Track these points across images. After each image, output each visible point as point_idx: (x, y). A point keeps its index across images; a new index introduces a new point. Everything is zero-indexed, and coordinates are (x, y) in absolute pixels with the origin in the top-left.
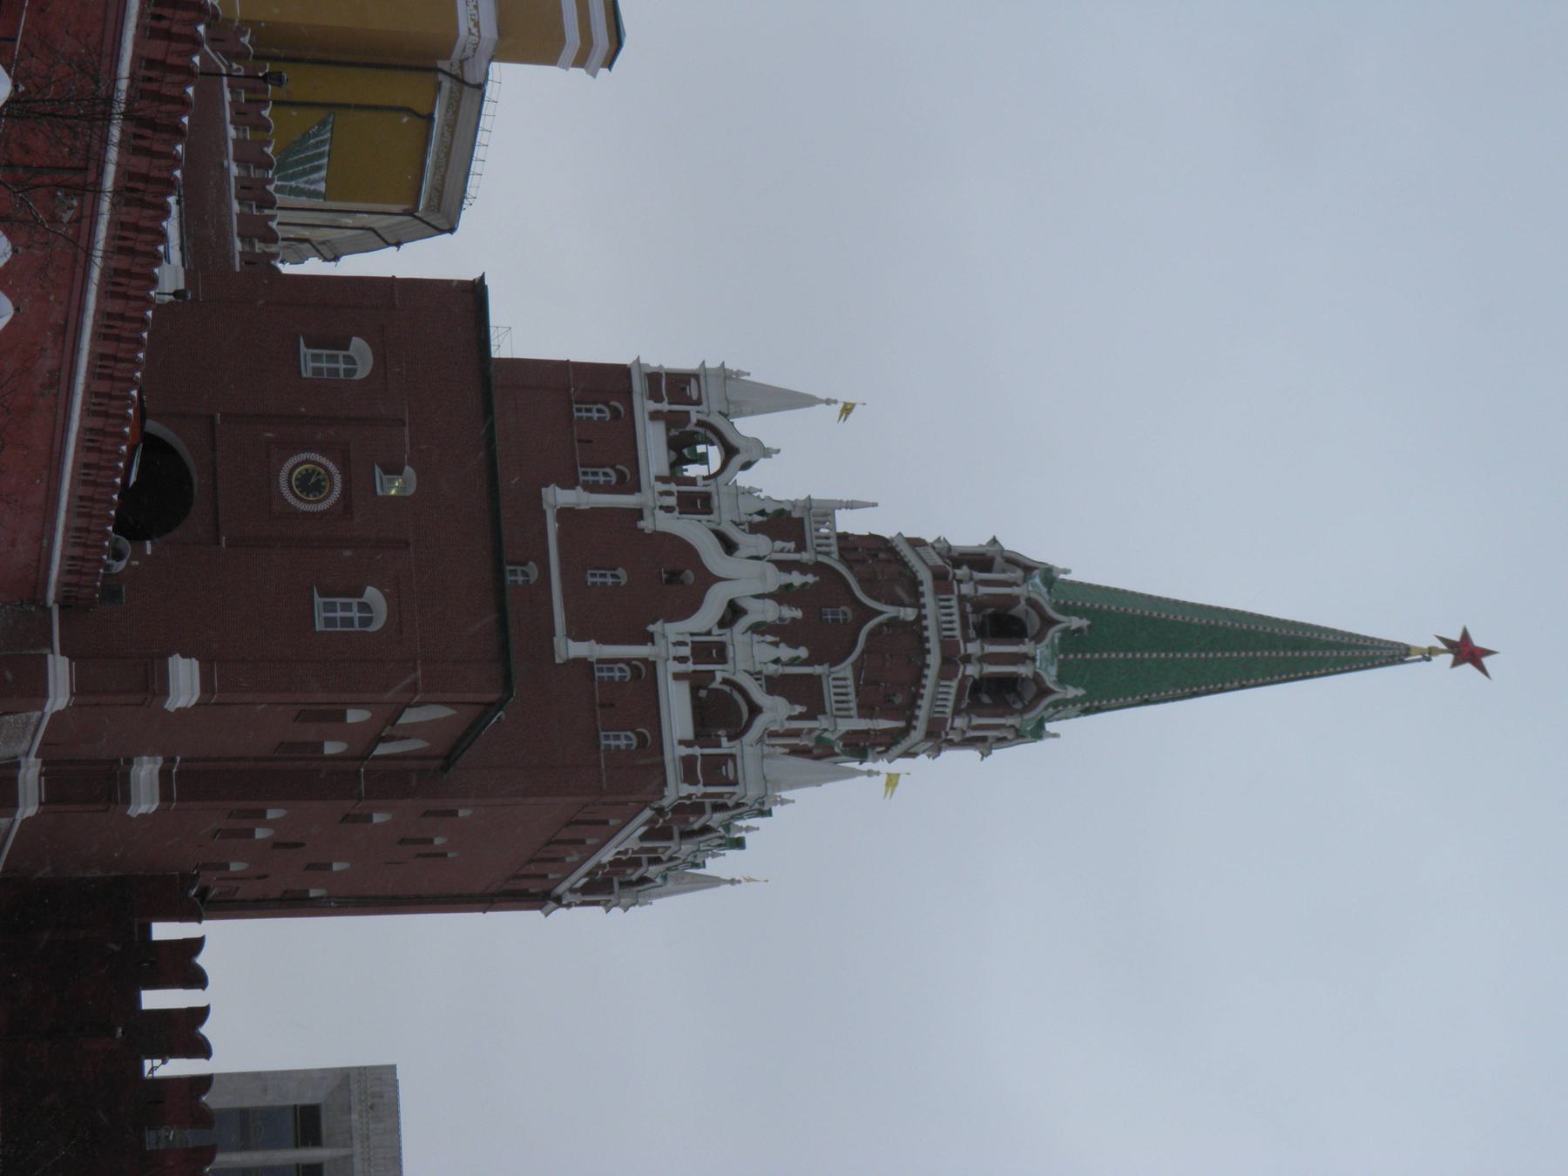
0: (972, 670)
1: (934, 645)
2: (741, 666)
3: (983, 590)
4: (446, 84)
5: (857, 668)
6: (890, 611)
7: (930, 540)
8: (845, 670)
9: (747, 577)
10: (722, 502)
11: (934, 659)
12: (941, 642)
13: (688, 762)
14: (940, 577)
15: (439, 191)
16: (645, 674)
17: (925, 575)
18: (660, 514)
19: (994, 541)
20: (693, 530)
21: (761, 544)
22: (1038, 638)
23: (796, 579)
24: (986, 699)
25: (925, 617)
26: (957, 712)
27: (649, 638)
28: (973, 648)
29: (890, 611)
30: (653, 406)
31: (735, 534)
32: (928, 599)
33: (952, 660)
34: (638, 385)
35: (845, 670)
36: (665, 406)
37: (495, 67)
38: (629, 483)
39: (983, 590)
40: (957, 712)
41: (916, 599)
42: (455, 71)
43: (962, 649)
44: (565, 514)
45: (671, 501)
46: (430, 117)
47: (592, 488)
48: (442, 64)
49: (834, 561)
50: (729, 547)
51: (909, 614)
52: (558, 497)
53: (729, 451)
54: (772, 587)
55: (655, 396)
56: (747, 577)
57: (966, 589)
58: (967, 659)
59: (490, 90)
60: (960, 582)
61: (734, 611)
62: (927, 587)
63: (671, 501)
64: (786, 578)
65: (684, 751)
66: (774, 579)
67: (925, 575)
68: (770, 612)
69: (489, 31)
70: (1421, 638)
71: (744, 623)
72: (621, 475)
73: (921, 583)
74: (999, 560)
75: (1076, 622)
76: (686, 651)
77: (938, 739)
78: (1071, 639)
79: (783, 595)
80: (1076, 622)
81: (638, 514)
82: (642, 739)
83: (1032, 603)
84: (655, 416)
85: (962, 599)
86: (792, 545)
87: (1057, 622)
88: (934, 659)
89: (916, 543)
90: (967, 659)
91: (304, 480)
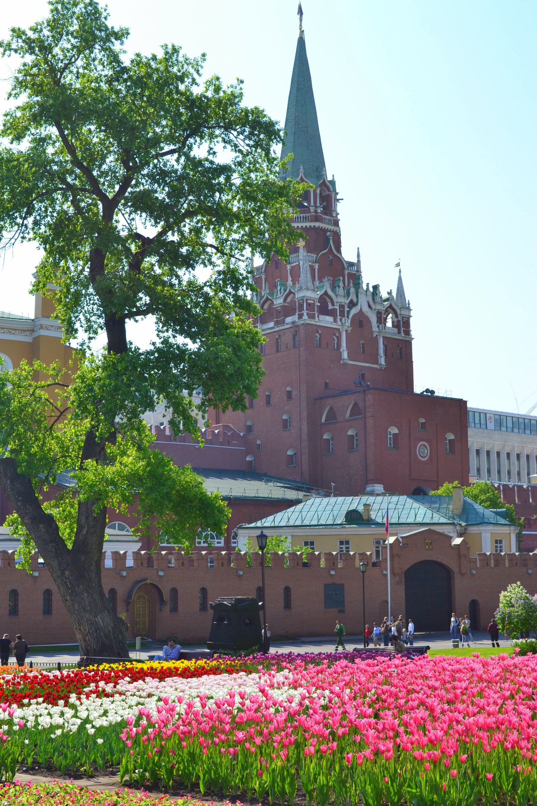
1: (313, 224)
11: (317, 224)
12: (311, 221)
24: (325, 204)
26: (331, 216)
28: (312, 209)
33: (317, 219)
58: (316, 212)
88: (317, 224)
90: (316, 212)
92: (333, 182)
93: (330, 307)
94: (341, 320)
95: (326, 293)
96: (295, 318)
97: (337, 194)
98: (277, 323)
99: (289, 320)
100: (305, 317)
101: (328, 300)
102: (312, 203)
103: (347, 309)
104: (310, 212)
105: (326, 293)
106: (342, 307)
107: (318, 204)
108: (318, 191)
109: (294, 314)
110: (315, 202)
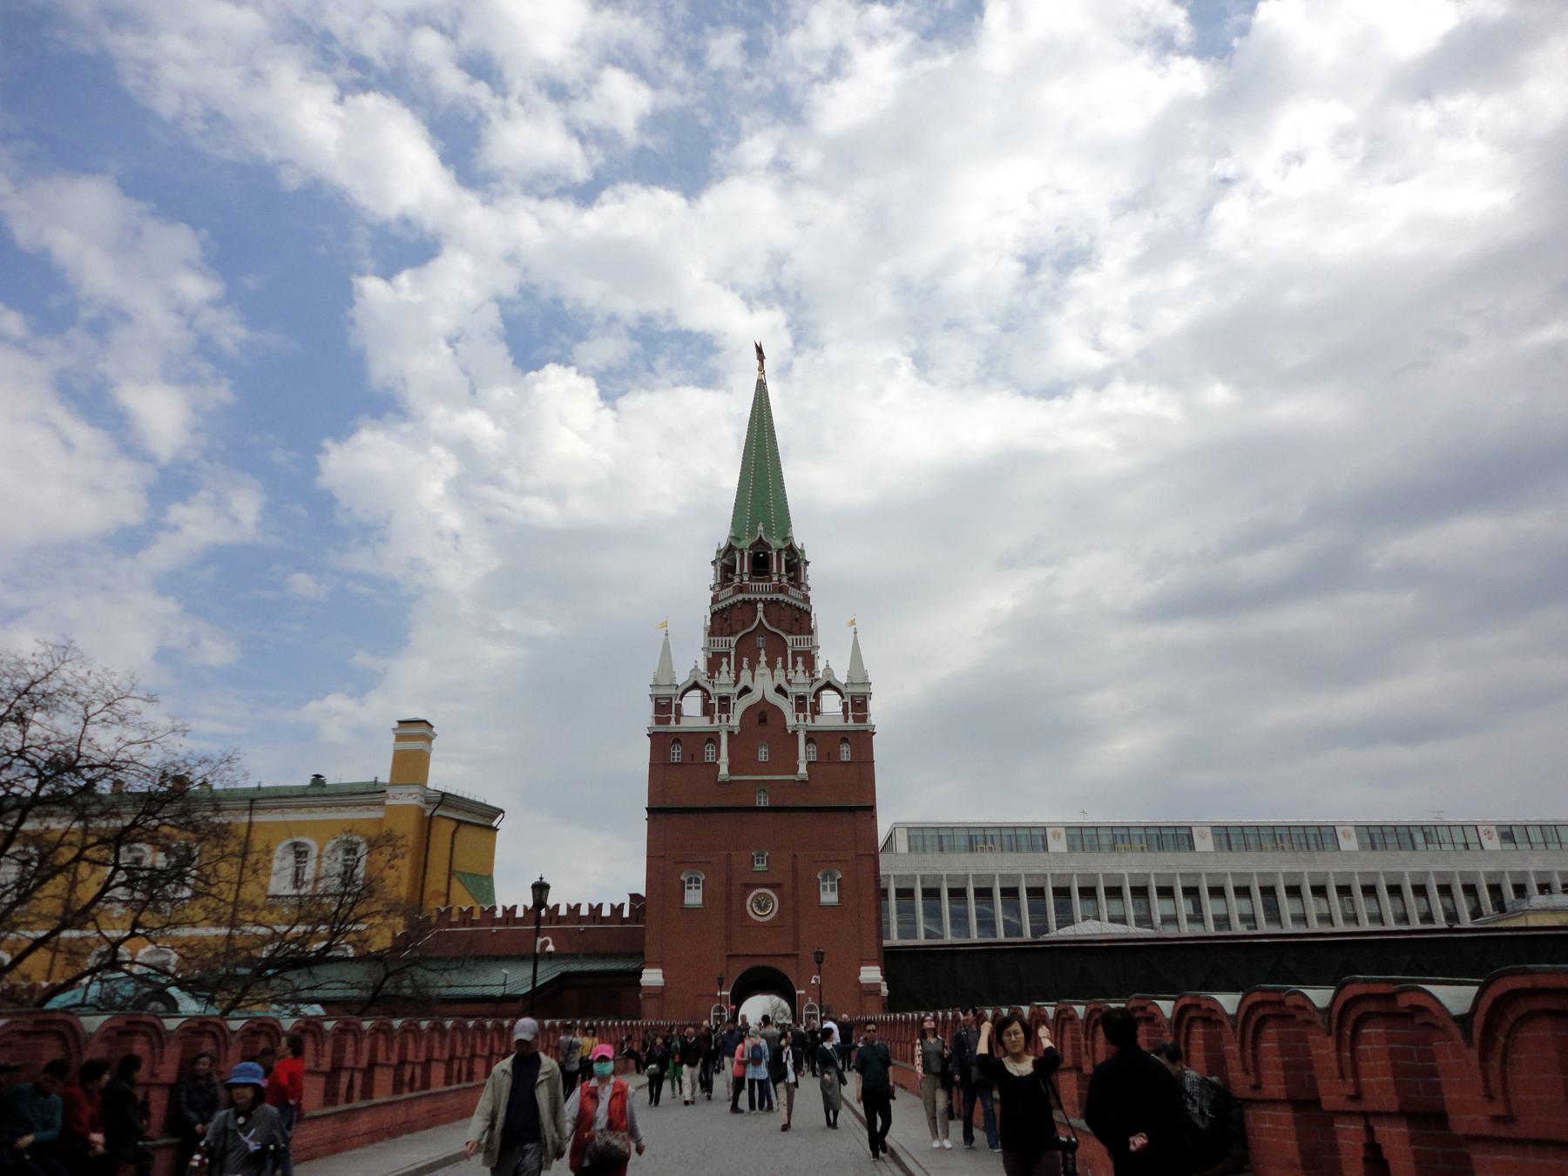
0: (784, 580)
1: (774, 597)
2: (807, 689)
4: (439, 812)
5: (790, 633)
6: (760, 615)
7: (711, 594)
8: (789, 639)
9: (763, 683)
10: (724, 691)
11: (781, 597)
13: (856, 719)
14: (741, 589)
15: (484, 816)
16: (811, 737)
17: (740, 597)
18: (731, 722)
19: (714, 563)
20: (740, 706)
21: (746, 676)
22: (769, 548)
23: (763, 659)
27: (794, 732)
28: (775, 578)
29: (760, 615)
30: (673, 722)
31: (740, 686)
33: (781, 590)
34: (662, 728)
35: (789, 639)
36: (673, 715)
37: (431, 784)
38: (713, 738)
41: (752, 604)
42: (432, 807)
43: (761, 584)
44: (732, 769)
45: (724, 717)
46: (459, 822)
47: (718, 756)
48: (428, 813)
49: (734, 640)
50: (746, 690)
51: (760, 606)
52: (724, 770)
53: (696, 686)
54: (768, 671)
55: (668, 721)
56: (763, 683)
57: (746, 578)
59: (441, 788)
61: (779, 690)
62: (747, 597)
63: (724, 717)
64: (763, 664)
65: (851, 721)
66: (762, 668)
67: (740, 597)
68: (779, 673)
69: (415, 789)
70: (755, 376)
71: (785, 686)
72: (710, 740)
75: (760, 527)
76: (801, 716)
77: (807, 599)
78: (767, 529)
79: (771, 665)
80: (760, 527)
81: (730, 733)
82: (845, 740)
84: (678, 721)
86: (725, 660)
88: (781, 597)
89: (715, 600)
91: (762, 908)
92: (803, 551)
97: (807, 563)
108: (784, 556)
110: (779, 568)
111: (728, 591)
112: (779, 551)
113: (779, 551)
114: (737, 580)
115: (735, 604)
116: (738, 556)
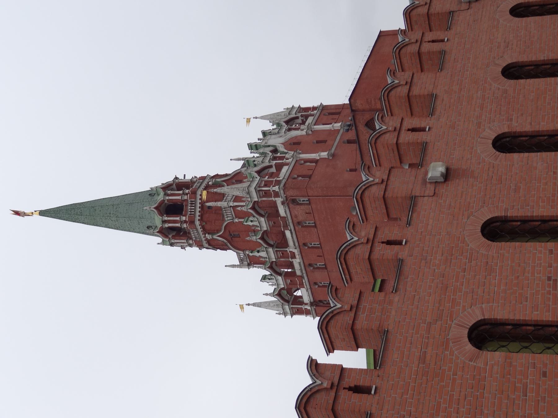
0: (187, 191)
3: (178, 219)
12: (196, 198)
14: (192, 222)
17: (197, 223)
25: (200, 207)
26: (195, 182)
28: (185, 197)
32: (198, 214)
39: (178, 219)
40: (195, 182)
57: (184, 218)
58: (187, 194)
60: (185, 222)
62: (198, 218)
67: (197, 223)
73: (199, 220)
74: (170, 236)
83: (161, 214)
85: (185, 216)
87: (154, 208)
90: (187, 194)
93: (273, 170)
94: (287, 159)
95: (259, 172)
96: (279, 201)
98: (286, 226)
99: (282, 211)
100: (276, 188)
101: (266, 171)
102: (179, 198)
103: (279, 155)
104: (187, 200)
105: (259, 172)
106: (275, 158)
107: (181, 192)
109: (275, 202)
111: (193, 234)
112: (166, 194)
113: (166, 194)
114: (185, 226)
115: (203, 227)
116: (167, 225)
